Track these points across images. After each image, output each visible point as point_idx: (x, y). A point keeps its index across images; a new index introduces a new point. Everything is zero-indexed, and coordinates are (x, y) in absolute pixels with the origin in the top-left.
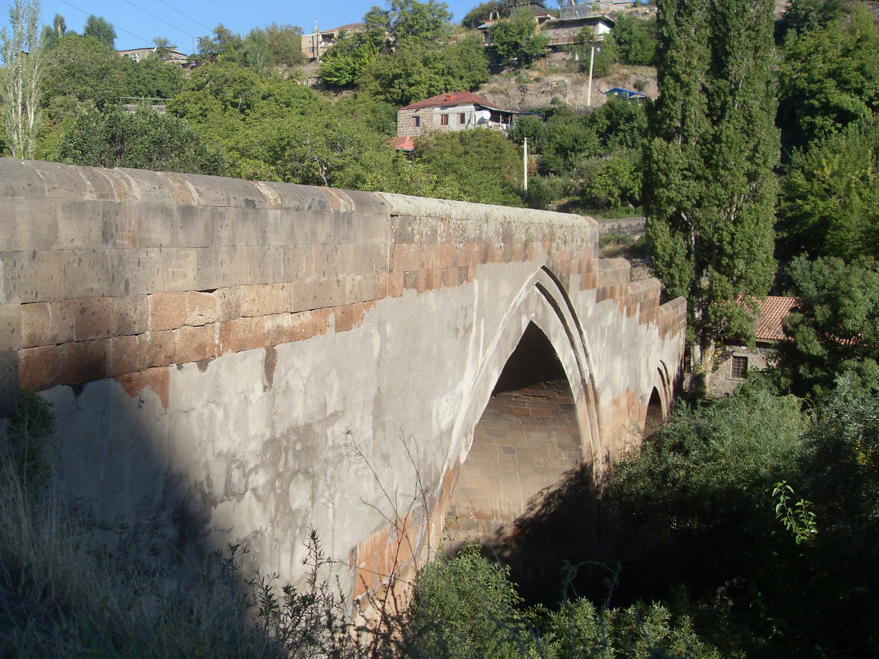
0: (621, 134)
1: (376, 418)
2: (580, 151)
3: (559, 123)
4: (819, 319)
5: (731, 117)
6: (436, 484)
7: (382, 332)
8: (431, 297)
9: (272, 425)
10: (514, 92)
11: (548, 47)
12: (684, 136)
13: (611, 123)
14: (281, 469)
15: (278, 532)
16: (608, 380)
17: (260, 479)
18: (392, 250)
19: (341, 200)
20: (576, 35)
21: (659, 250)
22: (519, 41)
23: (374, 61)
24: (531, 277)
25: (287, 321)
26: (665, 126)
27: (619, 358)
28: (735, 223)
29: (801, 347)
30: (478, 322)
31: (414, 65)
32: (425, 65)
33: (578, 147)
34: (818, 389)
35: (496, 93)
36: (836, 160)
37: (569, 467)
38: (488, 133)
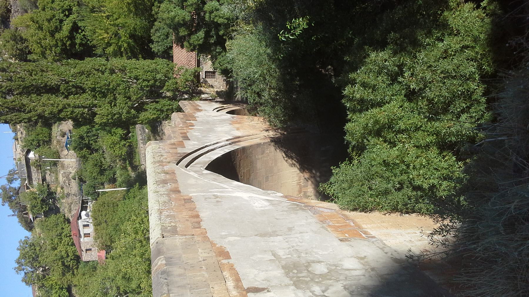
0: (91, 142)
1: (271, 236)
2: (101, 162)
3: (86, 175)
4: (186, 33)
5: (80, 83)
6: (298, 205)
7: (225, 237)
9: (287, 286)
10: (70, 200)
11: (43, 183)
12: (93, 107)
13: (85, 147)
14: (309, 279)
15: (342, 277)
16: (227, 133)
18: (182, 235)
19: (158, 263)
20: (35, 169)
21: (154, 116)
22: (40, 199)
23: (55, 277)
24: (183, 170)
25: (231, 284)
26: (88, 116)
28: (137, 80)
29: (201, 42)
31: (56, 255)
32: (56, 249)
33: (100, 164)
34: (221, 33)
35: (71, 209)
36: (99, 31)
37: (272, 148)
38: (94, 211)
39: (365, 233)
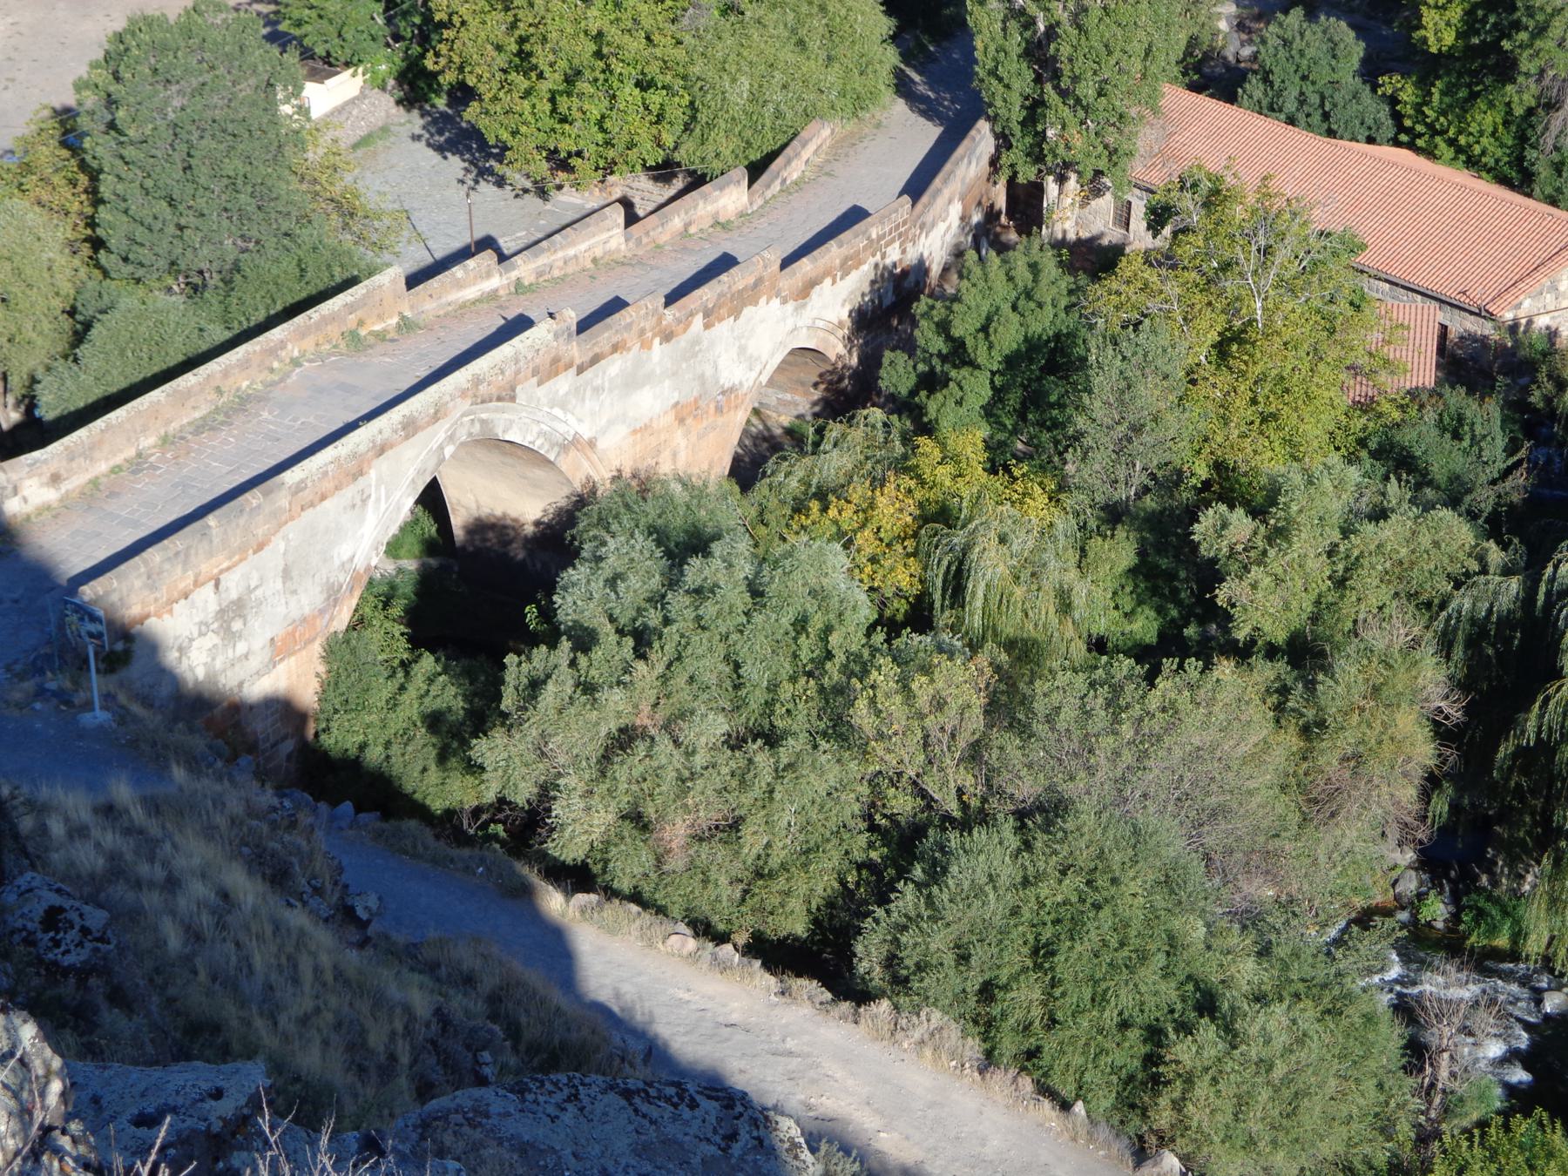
8: (326, 503)
17: (215, 626)
25: (225, 565)
30: (378, 487)
39: (282, 660)
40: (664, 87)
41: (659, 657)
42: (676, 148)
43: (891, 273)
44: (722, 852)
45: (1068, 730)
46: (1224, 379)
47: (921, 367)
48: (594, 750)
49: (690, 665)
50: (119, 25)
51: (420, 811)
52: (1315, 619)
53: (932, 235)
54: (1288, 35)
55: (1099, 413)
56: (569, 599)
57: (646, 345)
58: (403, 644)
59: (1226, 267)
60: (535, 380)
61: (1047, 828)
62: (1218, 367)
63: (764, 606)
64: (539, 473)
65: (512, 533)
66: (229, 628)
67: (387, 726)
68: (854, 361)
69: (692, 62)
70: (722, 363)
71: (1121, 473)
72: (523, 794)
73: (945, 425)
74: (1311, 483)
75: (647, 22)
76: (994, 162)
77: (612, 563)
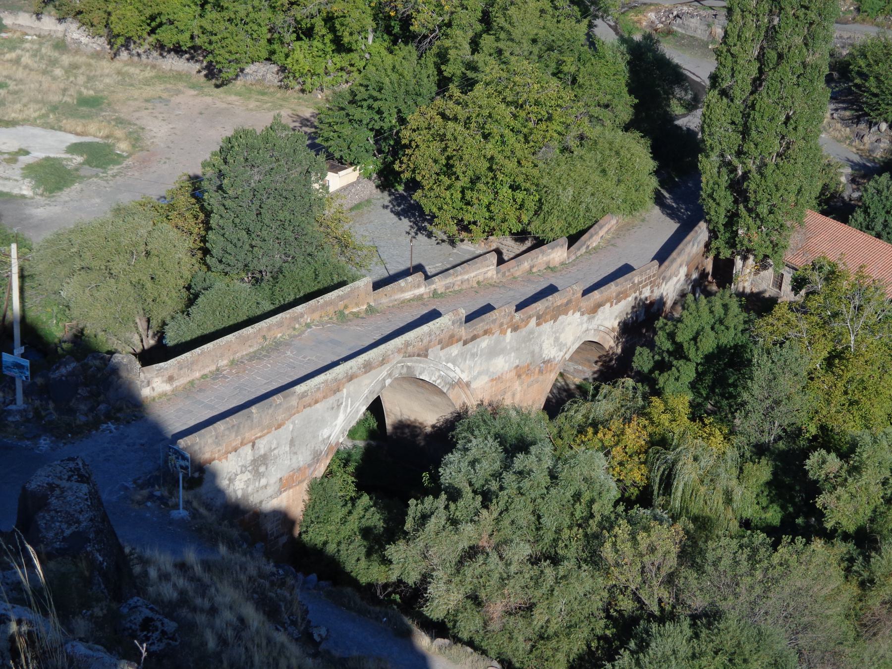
8: (318, 405)
17: (250, 468)
25: (259, 435)
27: (501, 356)
40: (525, 190)
41: (495, 509)
42: (529, 224)
43: (644, 303)
44: (521, 623)
45: (725, 571)
46: (830, 378)
47: (657, 357)
48: (454, 557)
49: (513, 514)
50: (229, 133)
51: (353, 582)
52: (872, 520)
53: (669, 283)
54: (880, 188)
55: (756, 391)
56: (448, 471)
57: (503, 332)
58: (352, 487)
59: (835, 315)
60: (439, 346)
61: (709, 626)
62: (827, 371)
63: (557, 484)
64: (437, 399)
65: (419, 431)
66: (258, 470)
67: (340, 534)
68: (619, 351)
69: (542, 177)
70: (545, 345)
71: (767, 426)
72: (412, 578)
73: (668, 391)
74: (875, 442)
75: (519, 154)
76: (707, 246)
77: (474, 453)
